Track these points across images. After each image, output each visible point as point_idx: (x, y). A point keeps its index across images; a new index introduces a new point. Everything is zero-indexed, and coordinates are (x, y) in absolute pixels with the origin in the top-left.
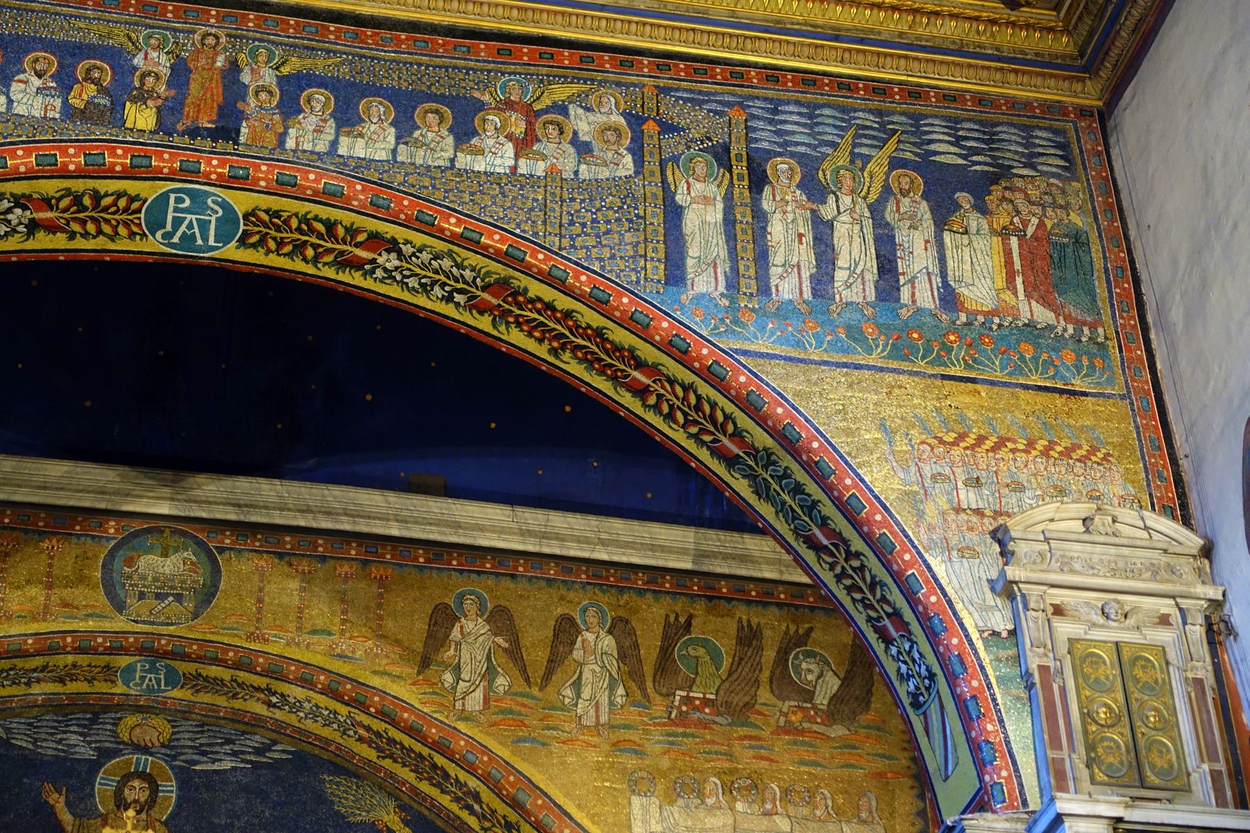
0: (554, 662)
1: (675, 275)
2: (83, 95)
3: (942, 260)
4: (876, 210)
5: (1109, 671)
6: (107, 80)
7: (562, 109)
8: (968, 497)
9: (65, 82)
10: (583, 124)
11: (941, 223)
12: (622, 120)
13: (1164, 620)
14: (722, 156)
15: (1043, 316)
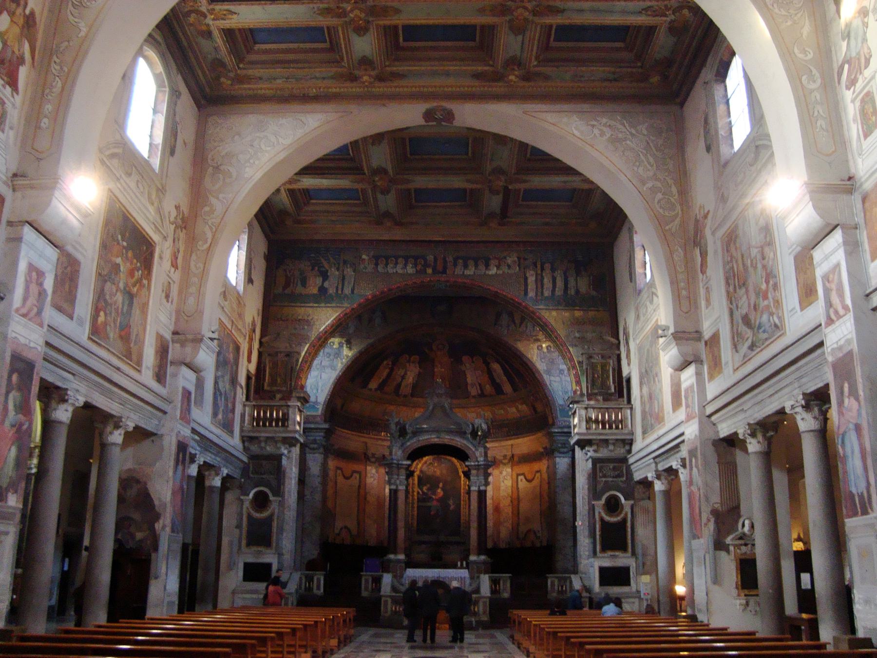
0: (521, 323)
1: (526, 293)
2: (419, 267)
3: (577, 284)
4: (565, 273)
5: (599, 368)
6: (423, 262)
7: (505, 258)
8: (577, 335)
9: (415, 265)
10: (509, 261)
11: (577, 275)
12: (516, 259)
13: (610, 357)
14: (535, 264)
15: (594, 293)
